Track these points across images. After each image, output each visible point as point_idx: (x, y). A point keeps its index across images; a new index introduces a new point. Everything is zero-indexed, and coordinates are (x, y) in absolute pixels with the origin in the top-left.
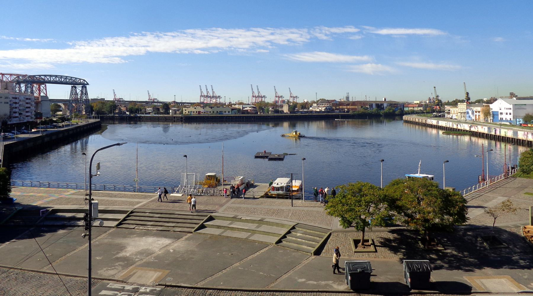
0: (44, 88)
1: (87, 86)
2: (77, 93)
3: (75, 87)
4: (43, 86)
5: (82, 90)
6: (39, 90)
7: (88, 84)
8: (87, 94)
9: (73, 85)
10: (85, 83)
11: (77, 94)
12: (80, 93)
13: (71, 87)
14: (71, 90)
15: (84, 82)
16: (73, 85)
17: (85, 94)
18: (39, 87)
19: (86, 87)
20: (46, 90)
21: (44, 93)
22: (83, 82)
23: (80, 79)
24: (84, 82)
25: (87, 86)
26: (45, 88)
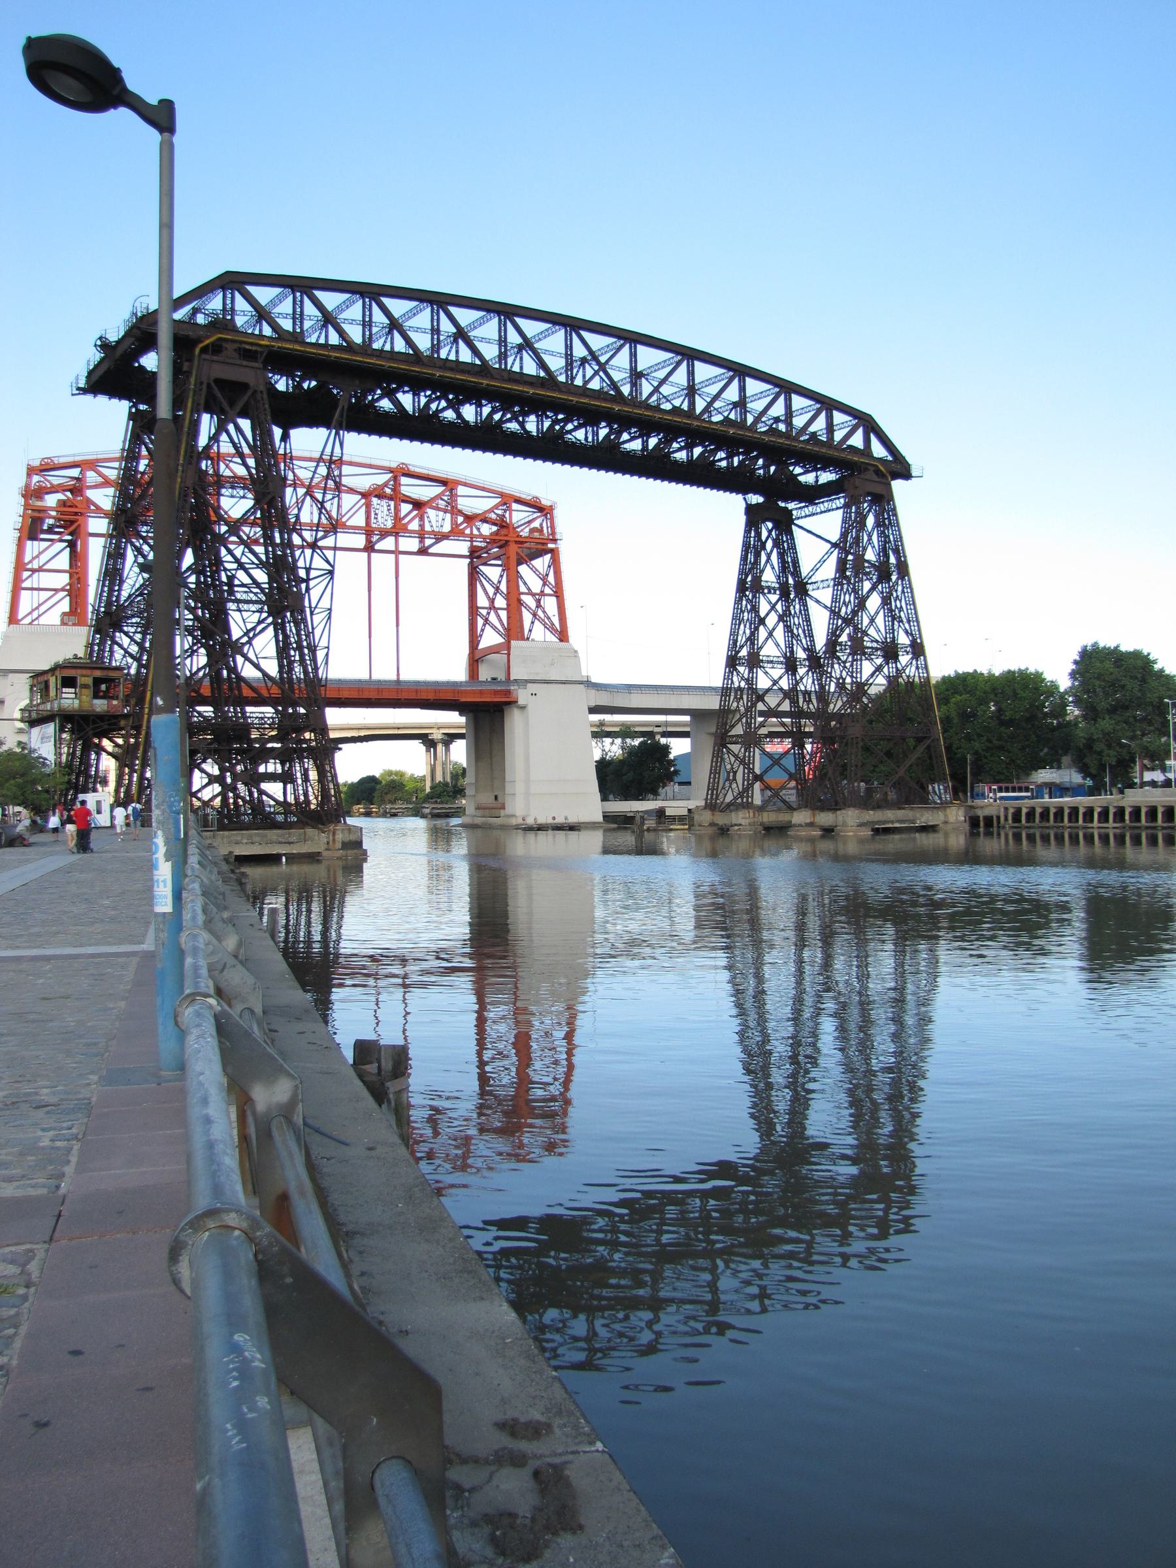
0: (545, 583)
1: (897, 485)
2: (805, 570)
3: (785, 523)
4: (542, 563)
5: (844, 535)
6: (515, 604)
7: (900, 469)
8: (903, 569)
9: (756, 499)
10: (878, 450)
11: (802, 589)
12: (829, 570)
13: (741, 519)
14: (746, 547)
15: (867, 441)
16: (756, 499)
17: (883, 573)
18: (514, 580)
19: (883, 501)
20: (558, 594)
21: (551, 628)
22: (857, 440)
23: (827, 405)
24: (867, 441)
25: (897, 485)
26: (551, 578)
